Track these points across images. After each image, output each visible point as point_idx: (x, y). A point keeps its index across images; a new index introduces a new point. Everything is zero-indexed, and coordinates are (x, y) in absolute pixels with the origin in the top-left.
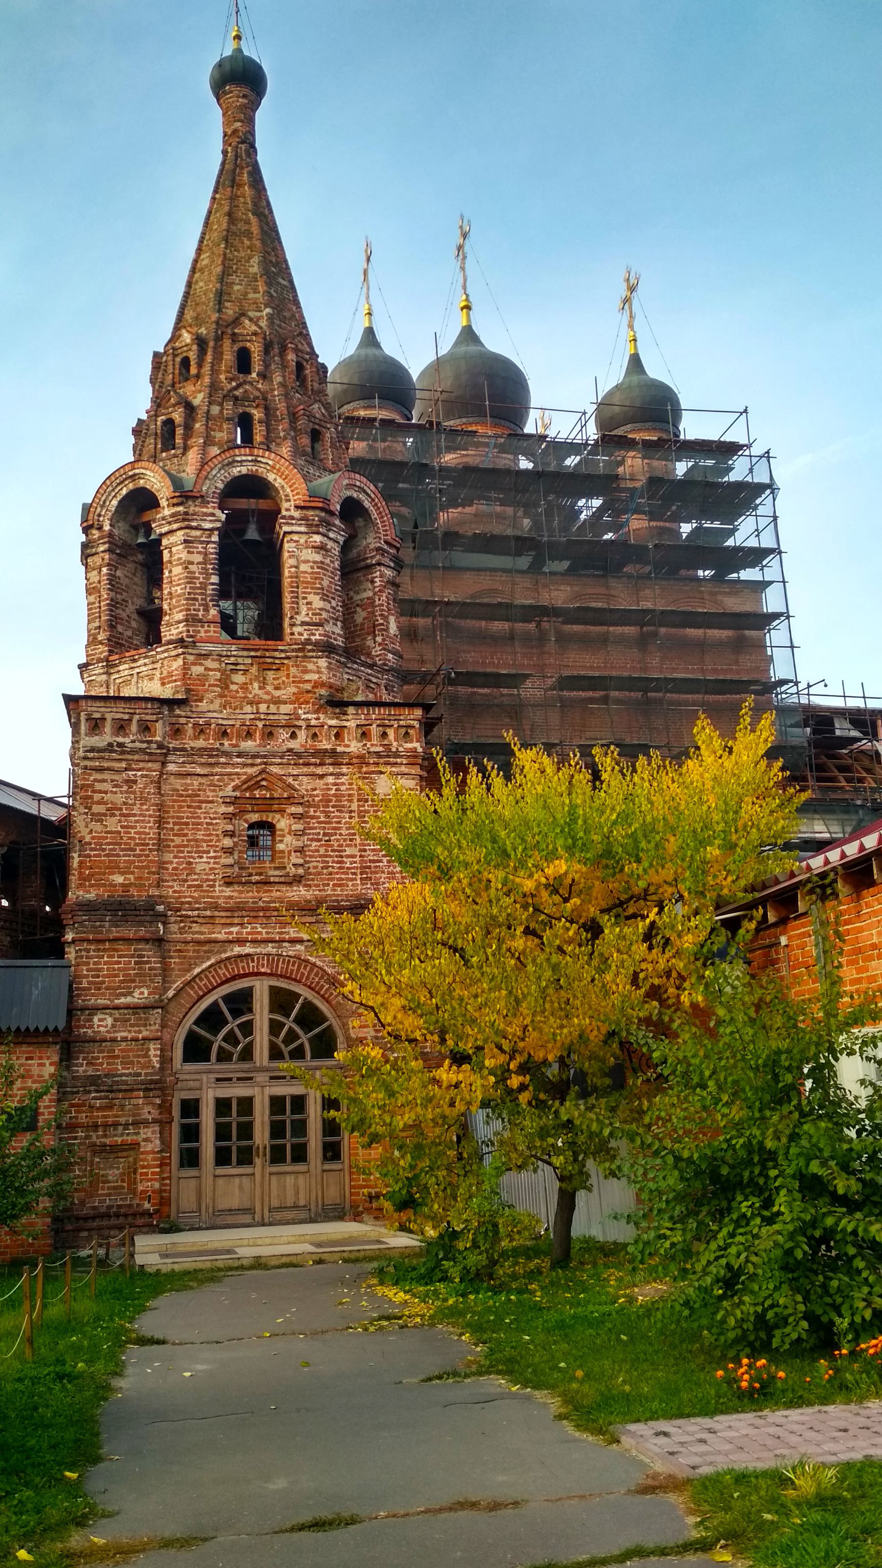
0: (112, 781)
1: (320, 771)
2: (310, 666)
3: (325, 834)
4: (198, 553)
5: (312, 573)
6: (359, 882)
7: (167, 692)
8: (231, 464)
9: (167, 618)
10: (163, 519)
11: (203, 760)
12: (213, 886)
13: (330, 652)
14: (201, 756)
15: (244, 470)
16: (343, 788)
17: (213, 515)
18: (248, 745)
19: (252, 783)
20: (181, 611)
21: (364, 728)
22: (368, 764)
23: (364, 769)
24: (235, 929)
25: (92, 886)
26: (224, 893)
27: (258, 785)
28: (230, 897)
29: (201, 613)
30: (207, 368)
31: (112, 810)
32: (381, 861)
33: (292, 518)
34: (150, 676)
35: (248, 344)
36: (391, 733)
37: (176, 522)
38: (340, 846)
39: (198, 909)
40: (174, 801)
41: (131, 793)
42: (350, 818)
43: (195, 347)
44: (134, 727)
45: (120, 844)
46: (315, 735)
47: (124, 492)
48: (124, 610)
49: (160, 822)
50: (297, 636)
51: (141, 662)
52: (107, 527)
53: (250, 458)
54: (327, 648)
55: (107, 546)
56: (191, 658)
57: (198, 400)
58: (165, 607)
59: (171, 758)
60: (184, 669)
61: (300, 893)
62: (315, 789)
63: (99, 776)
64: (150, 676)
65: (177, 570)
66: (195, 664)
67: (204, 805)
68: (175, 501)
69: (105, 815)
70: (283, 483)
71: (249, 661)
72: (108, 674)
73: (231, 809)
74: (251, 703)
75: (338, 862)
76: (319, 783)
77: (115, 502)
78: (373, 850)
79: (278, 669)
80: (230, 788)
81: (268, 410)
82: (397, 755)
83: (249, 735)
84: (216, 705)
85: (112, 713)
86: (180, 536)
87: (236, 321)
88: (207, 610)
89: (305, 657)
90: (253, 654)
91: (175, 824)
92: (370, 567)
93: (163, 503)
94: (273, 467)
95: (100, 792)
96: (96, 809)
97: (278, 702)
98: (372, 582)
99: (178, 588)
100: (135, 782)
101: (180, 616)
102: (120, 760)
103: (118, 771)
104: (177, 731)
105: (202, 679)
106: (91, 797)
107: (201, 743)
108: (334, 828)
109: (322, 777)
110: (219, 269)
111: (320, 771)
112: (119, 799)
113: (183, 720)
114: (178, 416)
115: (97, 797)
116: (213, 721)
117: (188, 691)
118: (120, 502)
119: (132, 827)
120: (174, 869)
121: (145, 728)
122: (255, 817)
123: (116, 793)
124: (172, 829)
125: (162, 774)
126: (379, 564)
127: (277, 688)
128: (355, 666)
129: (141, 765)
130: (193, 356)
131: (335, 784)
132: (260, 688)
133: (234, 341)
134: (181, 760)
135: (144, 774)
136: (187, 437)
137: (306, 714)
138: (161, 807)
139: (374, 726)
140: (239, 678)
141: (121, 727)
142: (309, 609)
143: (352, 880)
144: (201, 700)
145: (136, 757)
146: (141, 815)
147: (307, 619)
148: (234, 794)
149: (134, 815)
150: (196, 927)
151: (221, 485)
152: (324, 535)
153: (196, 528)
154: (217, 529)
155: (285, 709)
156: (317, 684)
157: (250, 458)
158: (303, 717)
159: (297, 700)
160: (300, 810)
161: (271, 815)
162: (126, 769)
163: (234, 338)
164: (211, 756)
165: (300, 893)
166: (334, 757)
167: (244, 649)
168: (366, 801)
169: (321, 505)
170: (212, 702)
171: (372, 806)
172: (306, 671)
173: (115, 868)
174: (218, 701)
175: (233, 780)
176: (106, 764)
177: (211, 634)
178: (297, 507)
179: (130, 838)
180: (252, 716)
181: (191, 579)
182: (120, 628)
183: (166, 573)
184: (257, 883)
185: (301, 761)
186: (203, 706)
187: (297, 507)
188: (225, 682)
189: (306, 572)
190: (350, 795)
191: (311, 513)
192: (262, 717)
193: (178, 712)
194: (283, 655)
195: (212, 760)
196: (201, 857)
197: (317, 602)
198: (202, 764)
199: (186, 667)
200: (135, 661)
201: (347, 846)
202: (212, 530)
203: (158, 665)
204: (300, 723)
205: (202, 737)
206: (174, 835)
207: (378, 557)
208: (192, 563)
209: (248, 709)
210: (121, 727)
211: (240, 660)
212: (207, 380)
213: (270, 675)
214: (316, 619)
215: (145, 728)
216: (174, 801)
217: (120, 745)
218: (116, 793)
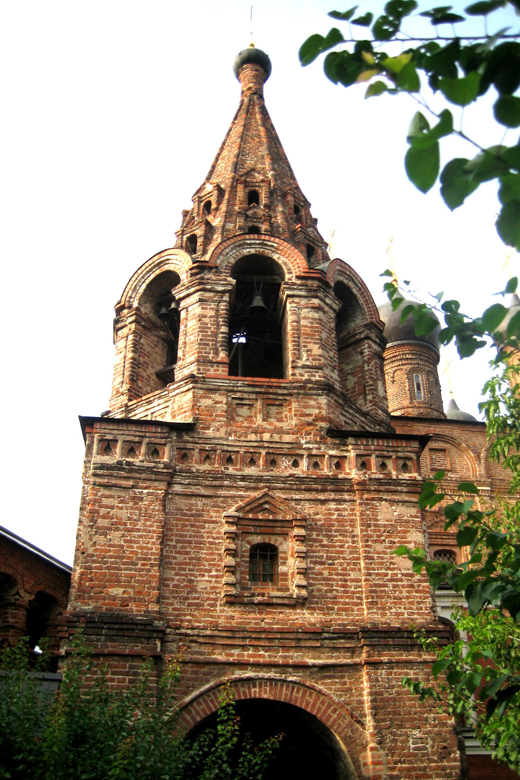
0: (119, 497)
1: (321, 497)
2: (312, 403)
3: (328, 558)
4: (210, 309)
5: (310, 327)
6: (364, 606)
8: (242, 245)
11: (207, 483)
12: (214, 605)
13: (329, 391)
14: (206, 478)
15: (253, 251)
16: (344, 513)
17: (225, 280)
19: (256, 506)
20: (193, 354)
21: (363, 459)
22: (369, 491)
23: (366, 496)
24: (236, 652)
25: (90, 598)
27: (260, 508)
28: (232, 618)
29: (211, 356)
31: (115, 526)
32: (386, 586)
33: (295, 284)
35: (257, 188)
36: (390, 464)
37: (192, 286)
38: (344, 569)
39: (198, 628)
40: (179, 520)
41: (136, 509)
42: (354, 542)
45: (123, 557)
46: (316, 465)
47: (153, 276)
48: (145, 370)
49: (164, 539)
50: (298, 377)
51: (155, 403)
53: (258, 242)
54: (327, 388)
55: (133, 318)
56: (201, 392)
59: (178, 479)
60: (194, 401)
62: (317, 514)
63: (107, 492)
66: (202, 397)
67: (207, 525)
68: (193, 271)
69: (110, 529)
70: (286, 260)
71: (253, 396)
73: (233, 529)
74: (255, 432)
75: (343, 586)
76: (322, 508)
77: (144, 286)
78: (378, 574)
79: (281, 405)
80: (234, 508)
82: (397, 482)
83: (253, 462)
84: (222, 433)
85: (123, 436)
86: (196, 297)
88: (217, 353)
89: (306, 394)
90: (258, 390)
91: (177, 541)
92: (359, 341)
94: (277, 249)
95: (106, 507)
96: (102, 522)
97: (281, 431)
98: (362, 353)
100: (141, 499)
101: (193, 358)
102: (127, 478)
103: (125, 488)
104: (184, 455)
105: (210, 410)
106: (97, 512)
107: (206, 467)
108: (338, 552)
109: (324, 502)
110: (236, 152)
111: (321, 497)
112: (124, 514)
113: (190, 446)
115: (103, 511)
116: (218, 447)
118: (148, 286)
119: (135, 542)
120: (175, 586)
121: (154, 451)
122: (257, 539)
123: (121, 508)
124: (175, 547)
125: (167, 493)
126: (367, 338)
127: (280, 420)
128: (351, 411)
129: (148, 484)
130: (213, 199)
131: (337, 510)
132: (264, 420)
133: (245, 187)
134: (187, 481)
135: (151, 493)
138: (165, 525)
139: (373, 456)
140: (244, 411)
141: (131, 449)
142: (308, 355)
143: (357, 604)
144: (208, 428)
145: (143, 476)
146: (144, 530)
147: (308, 363)
148: (237, 514)
149: (138, 530)
150: (195, 647)
151: (233, 261)
152: (322, 300)
153: (210, 291)
154: (228, 291)
156: (319, 418)
157: (258, 242)
158: (305, 446)
159: (298, 431)
160: (302, 532)
161: (273, 538)
162: (133, 487)
163: (246, 184)
164: (215, 479)
166: (337, 485)
167: (249, 386)
168: (369, 526)
169: (318, 275)
170: (218, 430)
171: (375, 531)
172: (306, 407)
173: (117, 582)
174: (223, 430)
175: (236, 502)
177: (220, 372)
178: (298, 277)
179: (132, 552)
180: (256, 444)
181: (203, 329)
182: (140, 384)
183: (182, 327)
184: (259, 604)
185: (303, 487)
186: (210, 433)
187: (298, 277)
189: (306, 326)
190: (352, 521)
191: (310, 282)
192: (266, 445)
194: (286, 392)
195: (217, 483)
196: (203, 576)
197: (316, 350)
198: (207, 486)
199: (196, 399)
200: (150, 402)
201: (352, 570)
202: (223, 292)
204: (301, 452)
205: (208, 462)
206: (178, 553)
207: (366, 332)
208: (205, 317)
209: (252, 437)
210: (131, 449)
211: (245, 396)
214: (316, 363)
215: (154, 451)
216: (179, 520)
217: (129, 464)
218: (121, 508)
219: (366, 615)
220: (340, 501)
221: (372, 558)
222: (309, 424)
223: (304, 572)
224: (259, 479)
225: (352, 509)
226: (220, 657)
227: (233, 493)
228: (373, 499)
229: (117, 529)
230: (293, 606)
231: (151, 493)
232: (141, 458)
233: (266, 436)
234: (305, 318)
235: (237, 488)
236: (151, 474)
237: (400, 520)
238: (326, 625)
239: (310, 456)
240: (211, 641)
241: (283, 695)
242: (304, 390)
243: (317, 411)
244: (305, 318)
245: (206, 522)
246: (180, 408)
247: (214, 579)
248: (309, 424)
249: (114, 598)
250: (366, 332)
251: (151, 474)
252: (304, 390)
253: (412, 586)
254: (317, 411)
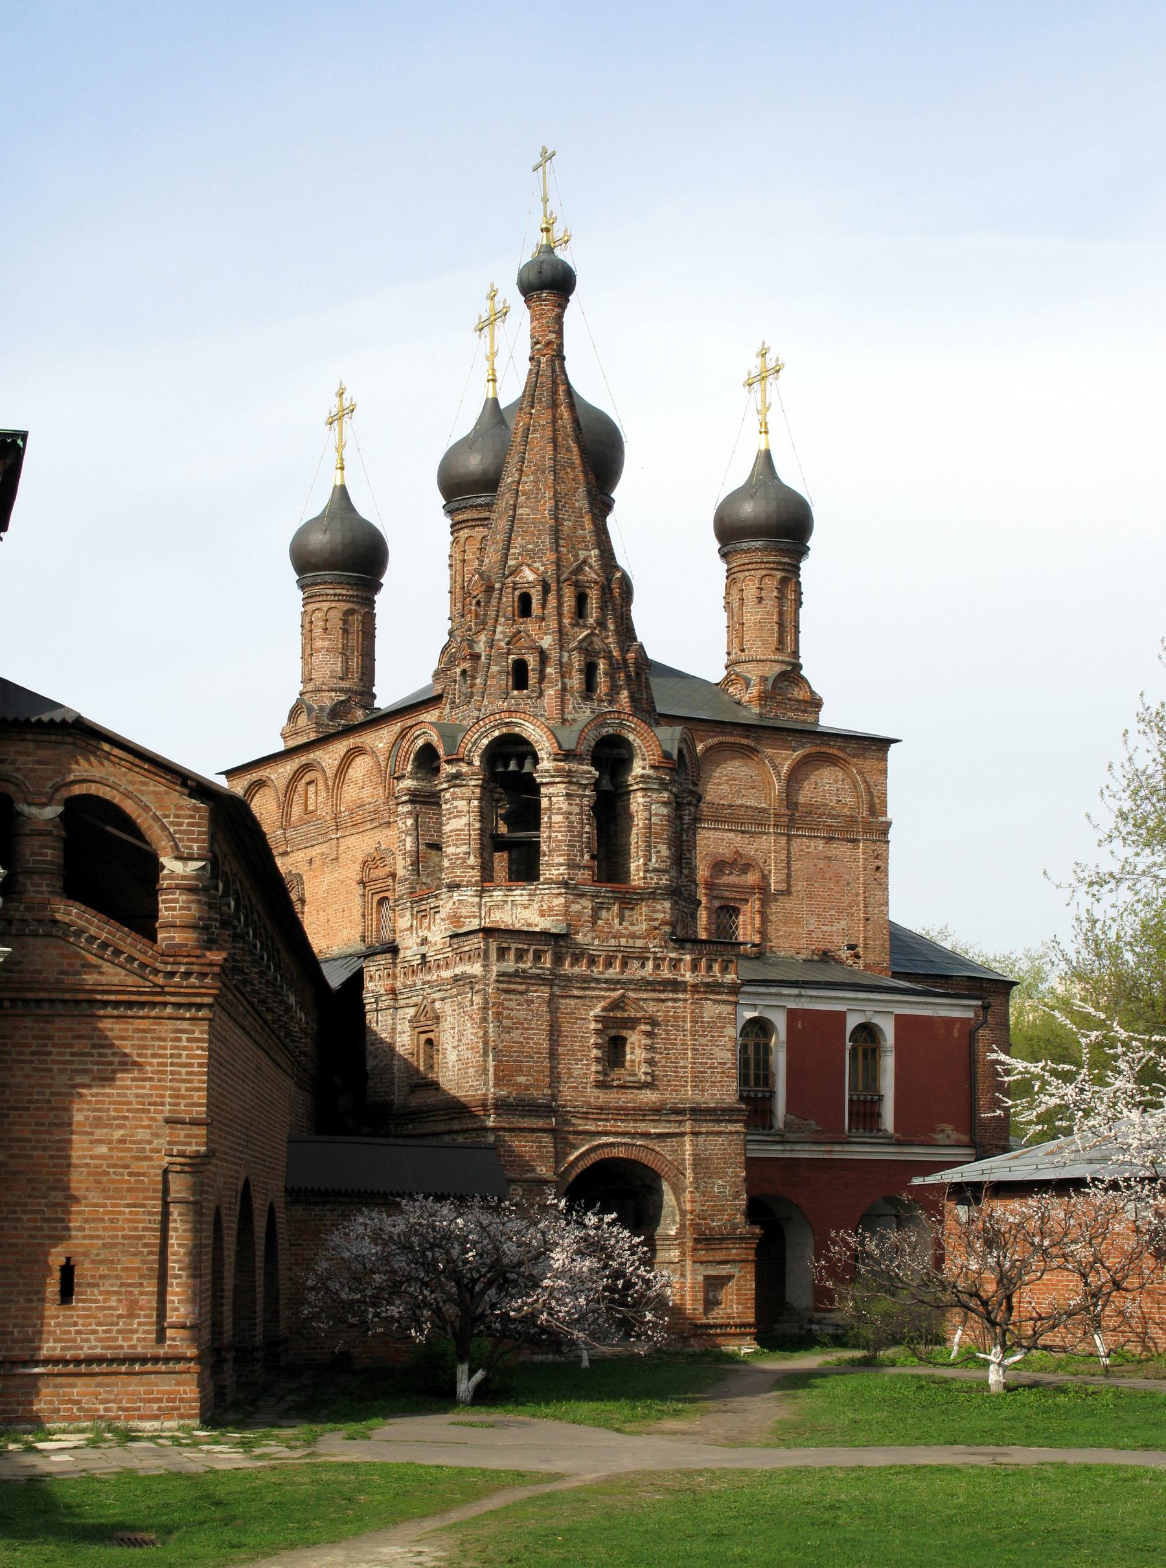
1: (662, 996)
7: (544, 924)
9: (546, 858)
10: (547, 771)
12: (585, 1088)
18: (612, 973)
19: (616, 1005)
22: (699, 992)
28: (598, 1097)
43: (539, 588)
44: (531, 956)
51: (518, 892)
52: (477, 762)
57: (547, 642)
58: (544, 847)
59: (557, 982)
63: (508, 997)
72: (481, 897)
73: (600, 1026)
74: (614, 937)
76: (663, 1006)
79: (632, 909)
82: (722, 985)
88: (582, 856)
93: (542, 754)
95: (508, 1009)
97: (633, 936)
99: (559, 835)
100: (532, 1002)
102: (521, 984)
103: (521, 993)
104: (558, 960)
105: (579, 914)
106: (501, 1013)
108: (673, 1044)
109: (663, 1001)
111: (662, 996)
112: (522, 1015)
114: (532, 661)
117: (569, 925)
121: (538, 957)
127: (632, 924)
129: (536, 988)
132: (621, 924)
143: (684, 1086)
148: (604, 1014)
149: (532, 1029)
153: (576, 783)
159: (647, 935)
160: (649, 1028)
164: (585, 982)
168: (697, 1022)
172: (655, 911)
173: (519, 1071)
174: (590, 935)
176: (513, 987)
181: (571, 828)
184: (617, 1087)
193: (561, 943)
199: (567, 905)
201: (682, 1059)
203: (537, 898)
207: (690, 798)
208: (571, 814)
209: (612, 942)
212: (554, 625)
213: (627, 913)
214: (663, 866)
217: (524, 971)
219: (689, 1095)
220: (675, 1000)
221: (697, 1050)
222: (656, 928)
223: (650, 1062)
224: (618, 982)
225: (682, 1006)
226: (590, 1127)
227: (596, 993)
228: (701, 999)
229: (517, 1028)
230: (639, 1088)
232: (529, 965)
233: (623, 941)
234: (656, 815)
235: (601, 989)
236: (540, 980)
237: (719, 1017)
238: (664, 1103)
239: (655, 959)
241: (633, 1154)
242: (652, 895)
243: (662, 915)
244: (656, 815)
245: (577, 1019)
246: (551, 909)
247: (583, 1065)
248: (656, 928)
249: (519, 1085)
250: (690, 798)
251: (540, 980)
252: (652, 895)
253: (723, 1072)
254: (662, 915)
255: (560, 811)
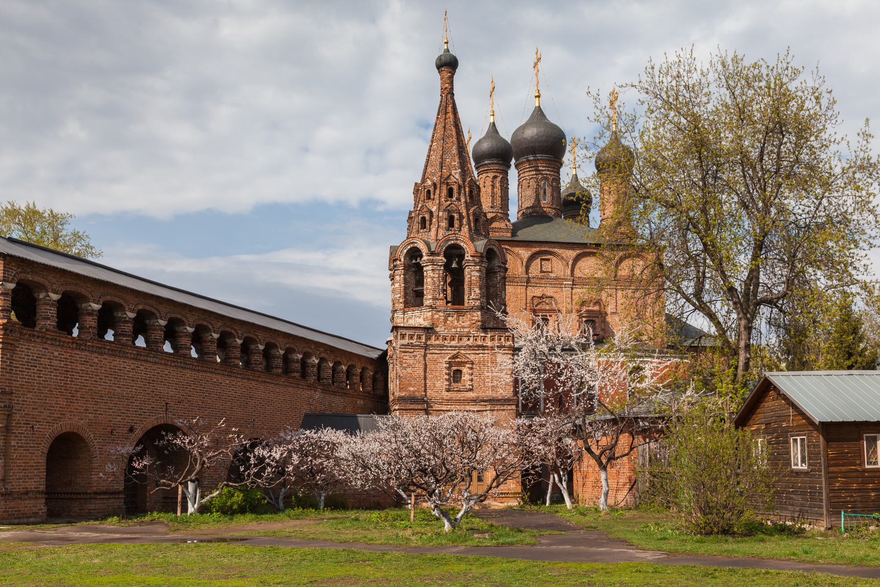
18: (453, 343)
19: (455, 357)
26: (445, 395)
27: (457, 357)
30: (437, 196)
31: (409, 366)
34: (418, 318)
36: (503, 339)
49: (425, 371)
61: (471, 395)
64: (418, 318)
65: (429, 280)
76: (477, 356)
81: (460, 214)
82: (504, 347)
85: (408, 332)
86: (430, 268)
87: (448, 177)
92: (496, 272)
96: (404, 365)
97: (463, 327)
101: (430, 297)
105: (438, 319)
107: (437, 342)
112: (411, 362)
114: (427, 216)
121: (419, 337)
122: (455, 368)
130: (432, 189)
136: (431, 224)
137: (473, 332)
138: (426, 365)
140: (450, 319)
155: (466, 330)
159: (469, 327)
165: (471, 395)
166: (483, 347)
173: (411, 385)
181: (434, 283)
188: (446, 320)
197: (478, 291)
199: (432, 315)
213: (461, 318)
215: (419, 337)
219: (489, 394)
223: (472, 380)
225: (486, 356)
231: (420, 353)
238: (478, 397)
240: (441, 404)
242: (472, 309)
252: (472, 309)
255: (432, 276)
